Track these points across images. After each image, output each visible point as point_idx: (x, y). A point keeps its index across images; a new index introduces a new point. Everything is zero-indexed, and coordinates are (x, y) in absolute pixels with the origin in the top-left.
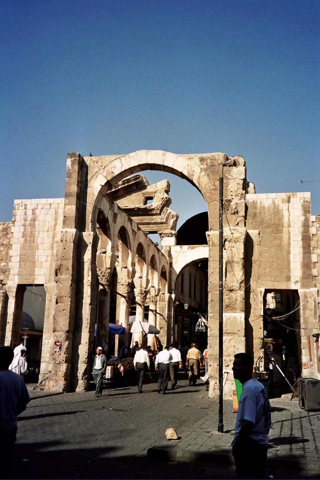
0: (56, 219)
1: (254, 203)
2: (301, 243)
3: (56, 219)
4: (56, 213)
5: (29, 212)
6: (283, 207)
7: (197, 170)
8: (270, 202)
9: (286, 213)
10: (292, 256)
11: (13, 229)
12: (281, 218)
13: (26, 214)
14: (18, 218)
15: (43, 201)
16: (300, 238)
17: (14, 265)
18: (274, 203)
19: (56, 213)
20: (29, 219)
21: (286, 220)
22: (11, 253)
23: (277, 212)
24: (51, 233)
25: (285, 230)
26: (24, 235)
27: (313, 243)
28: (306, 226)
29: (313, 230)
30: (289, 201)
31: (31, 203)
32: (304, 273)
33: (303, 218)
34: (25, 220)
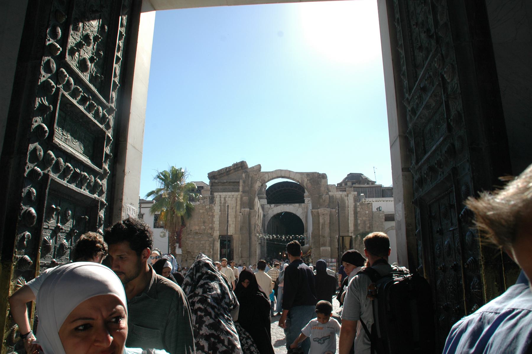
0: (236, 203)
1: (333, 196)
2: (353, 215)
3: (236, 203)
4: (236, 199)
5: (222, 199)
6: (346, 198)
7: (306, 180)
8: (340, 196)
9: (347, 202)
10: (349, 221)
11: (215, 208)
12: (345, 204)
13: (220, 200)
14: (216, 202)
15: (229, 193)
16: (353, 213)
17: (217, 225)
18: (341, 196)
19: (236, 199)
20: (223, 202)
21: (347, 204)
22: (214, 219)
23: (343, 200)
24: (234, 210)
25: (346, 209)
26: (220, 211)
27: (358, 215)
28: (355, 207)
29: (358, 209)
30: (348, 196)
31: (223, 194)
32: (355, 228)
33: (354, 204)
34: (221, 203)
